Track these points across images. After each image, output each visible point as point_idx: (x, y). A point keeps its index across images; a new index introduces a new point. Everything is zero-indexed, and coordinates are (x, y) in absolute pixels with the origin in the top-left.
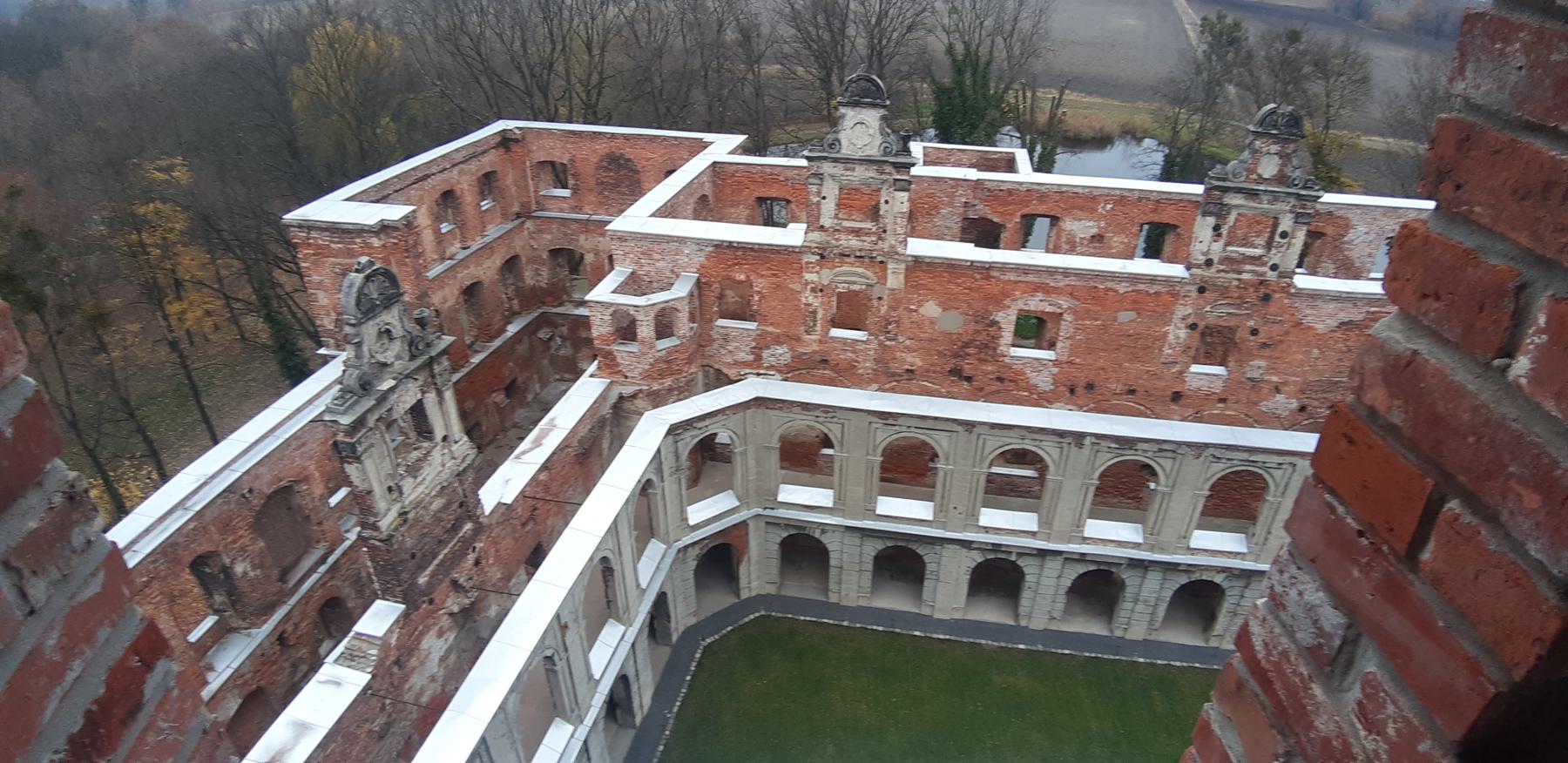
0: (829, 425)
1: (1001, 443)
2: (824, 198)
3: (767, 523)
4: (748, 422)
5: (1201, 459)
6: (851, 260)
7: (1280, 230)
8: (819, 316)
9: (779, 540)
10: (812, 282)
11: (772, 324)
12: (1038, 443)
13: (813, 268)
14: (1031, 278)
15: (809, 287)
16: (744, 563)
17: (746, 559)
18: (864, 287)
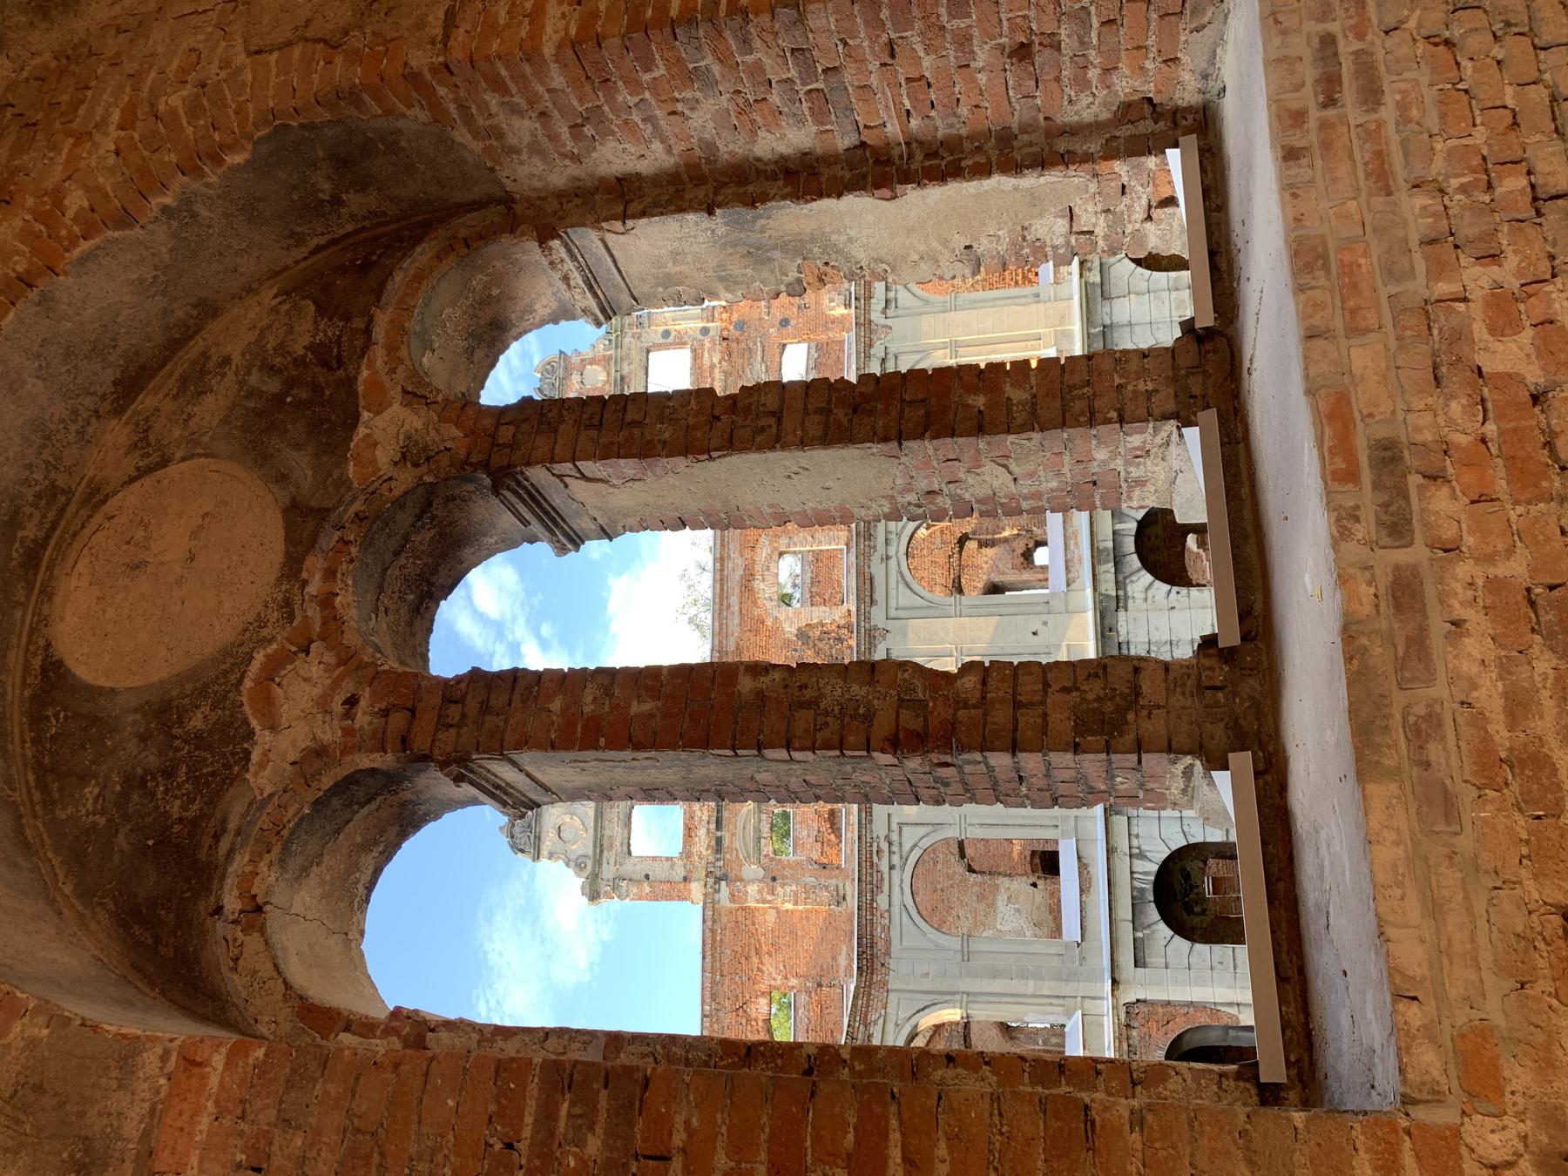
0: (907, 847)
1: (901, 586)
2: (647, 877)
3: (1139, 962)
4: (911, 988)
5: (889, 322)
6: (725, 834)
7: (662, 341)
8: (810, 880)
9: (1181, 944)
10: (760, 892)
11: (834, 959)
12: (893, 536)
13: (739, 891)
14: (734, 600)
15: (769, 898)
16: (1241, 1017)
17: (1233, 1011)
18: (764, 816)
